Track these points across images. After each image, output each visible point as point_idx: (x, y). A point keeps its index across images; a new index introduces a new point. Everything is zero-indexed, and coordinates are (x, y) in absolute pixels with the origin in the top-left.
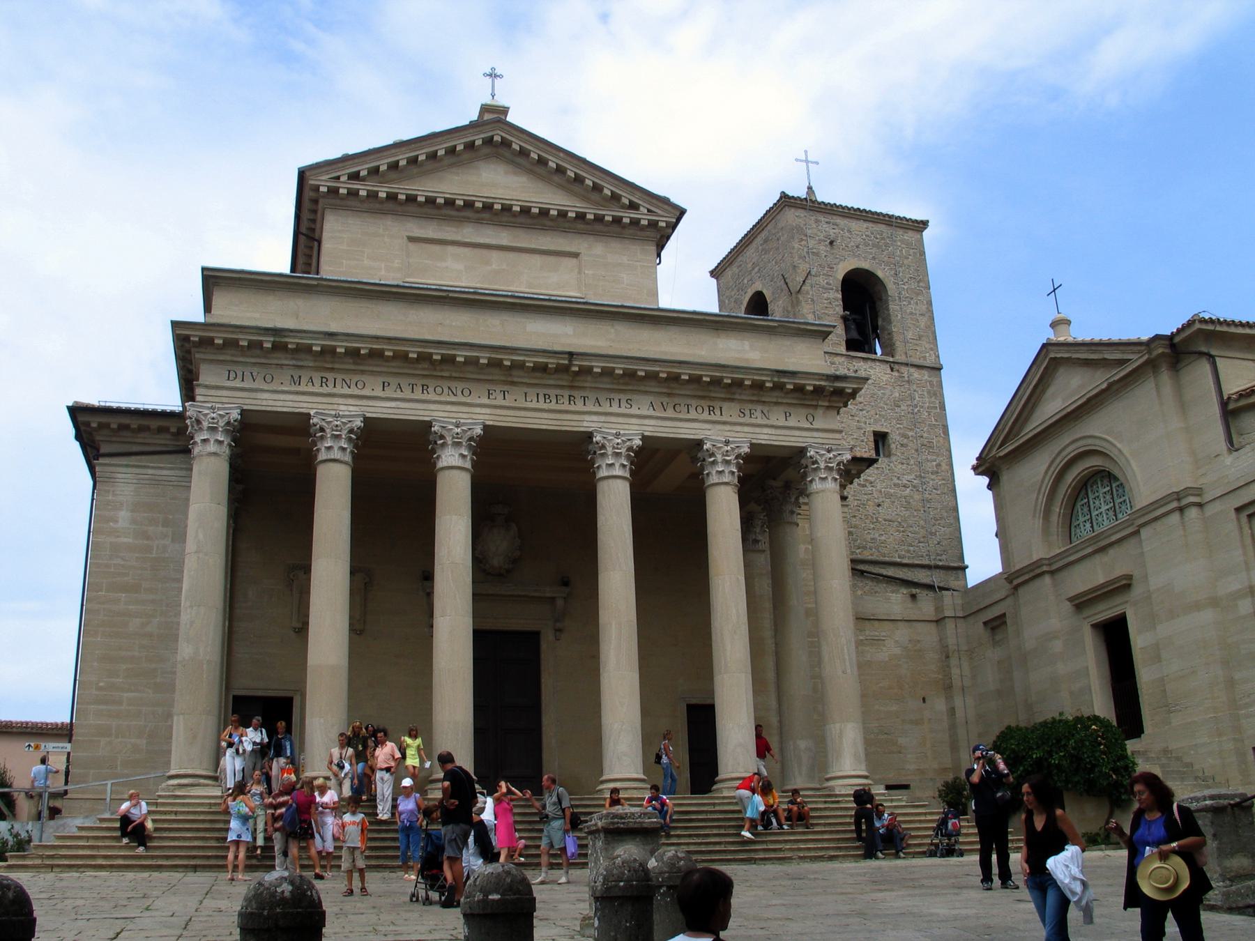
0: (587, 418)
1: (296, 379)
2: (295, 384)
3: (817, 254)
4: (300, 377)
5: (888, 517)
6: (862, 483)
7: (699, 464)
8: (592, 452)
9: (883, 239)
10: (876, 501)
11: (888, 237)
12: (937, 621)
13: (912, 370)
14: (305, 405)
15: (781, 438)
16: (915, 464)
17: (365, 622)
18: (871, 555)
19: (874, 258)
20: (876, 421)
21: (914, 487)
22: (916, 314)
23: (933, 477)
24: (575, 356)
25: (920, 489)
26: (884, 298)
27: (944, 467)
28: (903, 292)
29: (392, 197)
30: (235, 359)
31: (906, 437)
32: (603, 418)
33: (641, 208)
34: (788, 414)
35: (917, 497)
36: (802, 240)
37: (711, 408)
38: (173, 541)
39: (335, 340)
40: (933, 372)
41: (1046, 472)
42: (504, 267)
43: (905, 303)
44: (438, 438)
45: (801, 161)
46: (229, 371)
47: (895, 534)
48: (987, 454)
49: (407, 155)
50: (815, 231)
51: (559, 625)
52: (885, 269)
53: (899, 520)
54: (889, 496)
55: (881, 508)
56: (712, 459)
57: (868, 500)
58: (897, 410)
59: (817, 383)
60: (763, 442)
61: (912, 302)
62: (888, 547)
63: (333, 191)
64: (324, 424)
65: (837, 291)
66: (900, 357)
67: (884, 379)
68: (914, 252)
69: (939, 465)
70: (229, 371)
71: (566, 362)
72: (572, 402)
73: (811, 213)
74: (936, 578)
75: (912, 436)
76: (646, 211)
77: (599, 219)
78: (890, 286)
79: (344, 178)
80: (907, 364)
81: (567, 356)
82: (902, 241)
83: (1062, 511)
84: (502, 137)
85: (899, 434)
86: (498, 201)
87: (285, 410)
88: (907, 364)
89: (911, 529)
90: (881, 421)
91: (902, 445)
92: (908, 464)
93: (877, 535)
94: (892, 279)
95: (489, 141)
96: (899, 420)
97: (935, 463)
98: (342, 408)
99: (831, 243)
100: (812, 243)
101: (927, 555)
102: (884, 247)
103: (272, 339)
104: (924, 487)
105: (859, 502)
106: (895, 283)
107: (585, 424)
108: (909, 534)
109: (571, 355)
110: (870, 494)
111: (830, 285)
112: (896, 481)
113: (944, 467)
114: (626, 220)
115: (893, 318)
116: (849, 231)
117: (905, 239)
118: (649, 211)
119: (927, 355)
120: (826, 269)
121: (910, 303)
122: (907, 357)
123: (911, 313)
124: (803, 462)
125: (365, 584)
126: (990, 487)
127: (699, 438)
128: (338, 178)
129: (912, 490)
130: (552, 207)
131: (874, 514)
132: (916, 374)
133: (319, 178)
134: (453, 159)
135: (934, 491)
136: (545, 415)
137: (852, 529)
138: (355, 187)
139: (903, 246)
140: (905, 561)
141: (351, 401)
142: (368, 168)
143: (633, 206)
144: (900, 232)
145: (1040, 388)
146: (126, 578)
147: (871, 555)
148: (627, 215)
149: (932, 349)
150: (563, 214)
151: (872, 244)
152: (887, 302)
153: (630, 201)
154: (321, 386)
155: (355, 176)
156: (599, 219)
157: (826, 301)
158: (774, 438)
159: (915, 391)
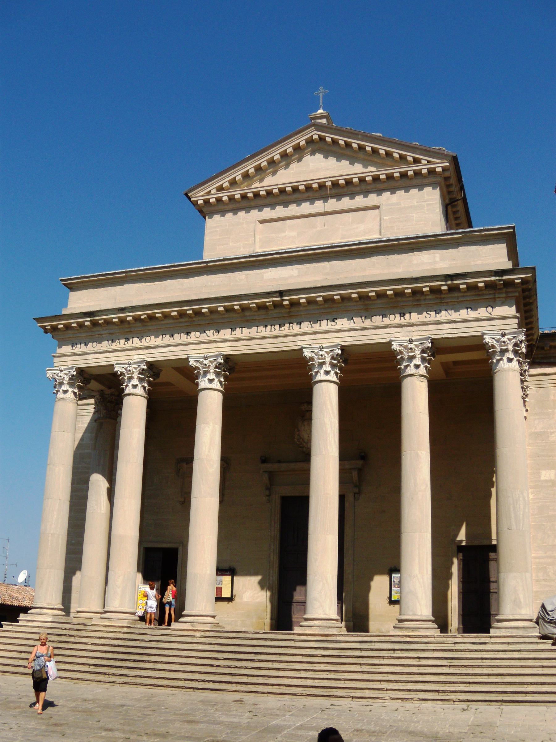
0: (300, 338)
2: (109, 345)
7: (395, 362)
15: (460, 330)
24: (284, 293)
29: (244, 197)
32: (313, 337)
33: (423, 162)
37: (402, 315)
39: (125, 313)
60: (446, 336)
63: (207, 202)
64: (124, 370)
71: (278, 299)
72: (291, 328)
76: (426, 162)
77: (390, 177)
81: (277, 295)
84: (318, 135)
95: (310, 141)
98: (135, 357)
103: (89, 319)
107: (299, 343)
109: (281, 293)
127: (384, 341)
128: (209, 192)
133: (198, 195)
136: (270, 341)
141: (141, 352)
142: (228, 181)
143: (416, 161)
150: (362, 180)
153: (414, 158)
154: (125, 344)
155: (221, 189)
156: (390, 177)
158: (455, 331)
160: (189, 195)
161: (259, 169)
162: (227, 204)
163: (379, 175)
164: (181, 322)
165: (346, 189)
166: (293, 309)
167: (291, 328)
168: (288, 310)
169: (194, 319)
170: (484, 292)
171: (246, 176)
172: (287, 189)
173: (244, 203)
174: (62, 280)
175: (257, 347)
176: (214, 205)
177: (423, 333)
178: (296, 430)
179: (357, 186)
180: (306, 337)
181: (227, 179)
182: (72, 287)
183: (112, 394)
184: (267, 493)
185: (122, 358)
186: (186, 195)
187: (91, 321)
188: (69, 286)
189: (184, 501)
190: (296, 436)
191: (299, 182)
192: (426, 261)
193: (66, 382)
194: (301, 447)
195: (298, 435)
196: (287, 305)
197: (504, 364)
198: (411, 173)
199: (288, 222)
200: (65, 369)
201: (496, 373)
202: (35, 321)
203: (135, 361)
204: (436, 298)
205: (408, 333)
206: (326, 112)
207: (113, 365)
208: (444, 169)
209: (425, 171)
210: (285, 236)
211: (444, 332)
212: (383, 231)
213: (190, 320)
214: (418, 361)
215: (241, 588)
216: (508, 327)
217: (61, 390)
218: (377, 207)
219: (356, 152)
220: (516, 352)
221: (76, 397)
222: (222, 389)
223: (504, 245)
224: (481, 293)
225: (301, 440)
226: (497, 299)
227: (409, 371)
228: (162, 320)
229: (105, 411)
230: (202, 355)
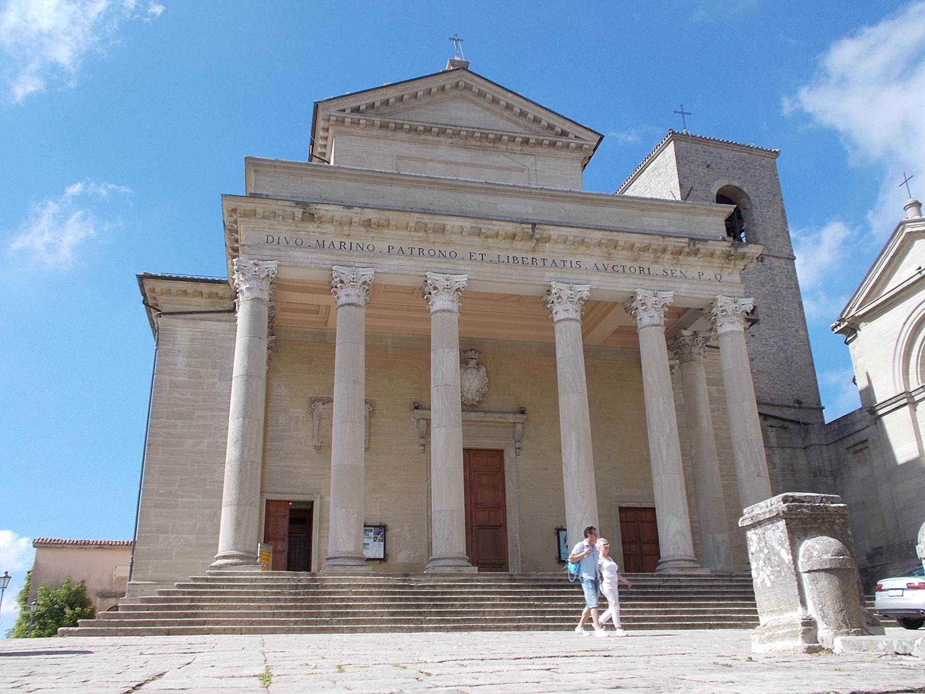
1: (320, 243)
8: (551, 302)
9: (746, 164)
11: (750, 163)
12: (805, 448)
13: (773, 259)
17: (369, 441)
21: (779, 347)
23: (793, 340)
24: (537, 227)
26: (748, 207)
27: (802, 332)
30: (273, 227)
31: (770, 309)
33: (570, 135)
34: (701, 274)
35: (782, 355)
37: (642, 269)
38: (220, 379)
40: (788, 261)
44: (432, 289)
47: (767, 382)
48: (847, 315)
51: (518, 445)
53: (769, 371)
56: (644, 307)
59: (724, 249)
61: (770, 210)
69: (797, 331)
73: (692, 144)
74: (801, 416)
75: (775, 309)
80: (769, 256)
85: (765, 307)
86: (464, 129)
88: (769, 256)
97: (794, 329)
100: (693, 167)
103: (302, 210)
104: (787, 347)
108: (778, 382)
111: (707, 197)
112: (764, 342)
113: (802, 332)
118: (576, 137)
120: (704, 185)
124: (714, 311)
125: (370, 412)
134: (430, 99)
139: (762, 169)
145: (896, 260)
146: (183, 408)
148: (560, 139)
149: (787, 245)
155: (356, 110)
159: (776, 275)
167: (692, 245)
184: (422, 441)
204: (674, 258)
209: (572, 145)
215: (394, 548)
224: (714, 260)
226: (725, 269)
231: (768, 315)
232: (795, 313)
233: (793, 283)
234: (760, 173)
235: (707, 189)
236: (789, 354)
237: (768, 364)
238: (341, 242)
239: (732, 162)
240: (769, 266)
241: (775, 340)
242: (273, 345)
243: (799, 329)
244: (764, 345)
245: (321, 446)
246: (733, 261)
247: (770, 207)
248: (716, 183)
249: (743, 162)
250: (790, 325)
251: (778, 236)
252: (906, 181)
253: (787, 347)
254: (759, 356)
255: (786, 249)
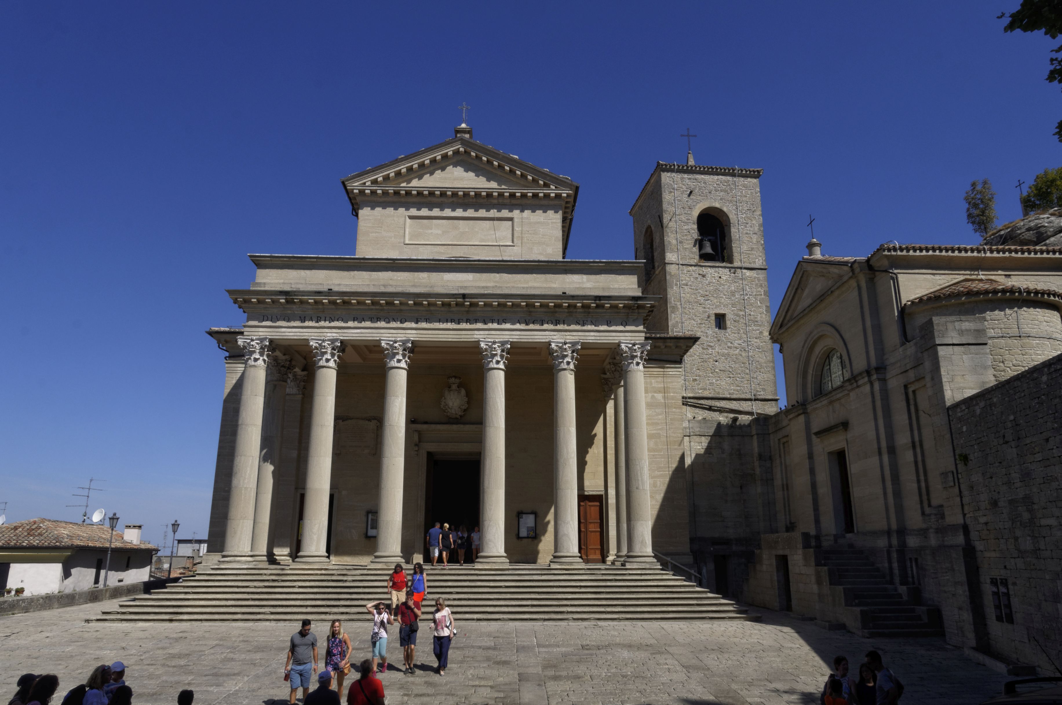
0: (476, 332)
1: (302, 319)
3: (679, 201)
4: (305, 317)
5: (723, 369)
6: (705, 347)
9: (729, 185)
10: (715, 358)
11: (733, 184)
13: (744, 271)
14: (307, 334)
16: (744, 333)
18: (710, 393)
19: (721, 199)
20: (717, 307)
22: (750, 234)
23: (756, 340)
25: (747, 349)
28: (741, 220)
29: (397, 193)
31: (738, 315)
32: (487, 332)
33: (552, 187)
34: (609, 322)
35: (744, 354)
36: (671, 192)
37: (558, 322)
41: (803, 347)
42: (467, 230)
43: (742, 227)
45: (684, 136)
46: (264, 316)
47: (727, 379)
49: (407, 165)
50: (681, 185)
52: (728, 206)
53: (731, 370)
54: (723, 355)
55: (717, 363)
57: (709, 358)
58: (733, 298)
59: (626, 302)
60: (591, 341)
61: (748, 226)
62: (722, 388)
63: (362, 192)
65: (694, 223)
66: (736, 264)
67: (725, 278)
68: (751, 192)
69: (761, 333)
70: (264, 316)
78: (732, 217)
79: (368, 184)
80: (741, 268)
82: (744, 186)
83: (814, 373)
85: (734, 313)
87: (295, 337)
88: (741, 268)
89: (739, 375)
90: (721, 306)
91: (735, 321)
92: (739, 333)
93: (714, 381)
94: (734, 211)
96: (733, 305)
97: (758, 331)
98: (329, 335)
99: (691, 192)
100: (677, 193)
101: (750, 392)
102: (729, 191)
105: (702, 360)
106: (735, 214)
107: (475, 336)
108: (738, 379)
109: (464, 296)
110: (711, 354)
112: (729, 344)
114: (541, 195)
115: (733, 238)
116: (705, 183)
117: (745, 184)
118: (556, 187)
119: (757, 260)
121: (746, 227)
122: (741, 263)
123: (747, 233)
125: (377, 426)
126: (781, 351)
128: (365, 183)
129: (740, 350)
130: (494, 190)
131: (713, 367)
132: (748, 273)
135: (757, 350)
137: (696, 378)
138: (374, 188)
139: (744, 188)
140: (734, 396)
141: (334, 330)
143: (546, 185)
144: (742, 179)
147: (710, 393)
148: (541, 191)
151: (721, 190)
152: (730, 226)
153: (544, 182)
155: (375, 182)
157: (686, 231)
158: (598, 338)
160: (346, 183)
161: (410, 169)
162: (380, 197)
163: (515, 193)
164: (372, 309)
165: (486, 200)
166: (472, 309)
168: (467, 309)
169: (385, 308)
170: (622, 311)
171: (398, 174)
172: (437, 193)
173: (396, 199)
174: (250, 256)
175: (440, 336)
176: (368, 196)
177: (573, 338)
178: (443, 398)
179: (495, 199)
180: (481, 332)
181: (381, 175)
182: (260, 263)
183: (286, 360)
184: (416, 448)
185: (316, 334)
186: (343, 183)
187: (286, 299)
188: (256, 262)
189: (340, 454)
190: (443, 403)
191: (447, 188)
192: (576, 281)
193: (258, 351)
194: (445, 412)
195: (445, 403)
196: (468, 305)
197: (633, 367)
198: (541, 195)
199: (434, 221)
200: (257, 339)
201: (628, 372)
202: (227, 294)
203: (329, 338)
205: (562, 337)
206: (468, 127)
207: (308, 340)
208: (568, 195)
210: (432, 233)
211: (590, 338)
212: (515, 240)
213: (381, 308)
214: (569, 359)
216: (637, 338)
217: (252, 358)
218: (511, 219)
219: (495, 168)
220: (641, 358)
221: (265, 363)
222: (406, 367)
223: (636, 276)
224: (619, 311)
225: (447, 407)
227: (564, 366)
228: (355, 305)
229: (279, 375)
230: (393, 339)
231: (735, 321)
232: (761, 317)
233: (762, 291)
234: (741, 192)
235: (689, 212)
236: (750, 354)
237: (730, 364)
238: (318, 317)
239: (715, 185)
240: (741, 277)
241: (740, 342)
242: (306, 378)
243: (763, 331)
244: (728, 347)
245: (340, 454)
246: (637, 311)
247: (747, 223)
248: (698, 205)
249: (725, 184)
250: (754, 328)
251: (752, 249)
252: (811, 223)
253: (750, 348)
254: (723, 358)
255: (759, 260)
